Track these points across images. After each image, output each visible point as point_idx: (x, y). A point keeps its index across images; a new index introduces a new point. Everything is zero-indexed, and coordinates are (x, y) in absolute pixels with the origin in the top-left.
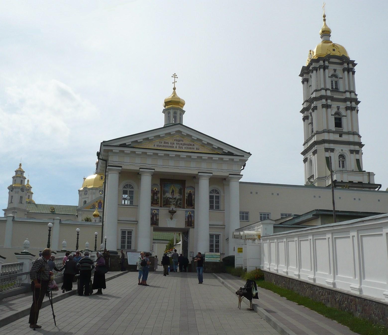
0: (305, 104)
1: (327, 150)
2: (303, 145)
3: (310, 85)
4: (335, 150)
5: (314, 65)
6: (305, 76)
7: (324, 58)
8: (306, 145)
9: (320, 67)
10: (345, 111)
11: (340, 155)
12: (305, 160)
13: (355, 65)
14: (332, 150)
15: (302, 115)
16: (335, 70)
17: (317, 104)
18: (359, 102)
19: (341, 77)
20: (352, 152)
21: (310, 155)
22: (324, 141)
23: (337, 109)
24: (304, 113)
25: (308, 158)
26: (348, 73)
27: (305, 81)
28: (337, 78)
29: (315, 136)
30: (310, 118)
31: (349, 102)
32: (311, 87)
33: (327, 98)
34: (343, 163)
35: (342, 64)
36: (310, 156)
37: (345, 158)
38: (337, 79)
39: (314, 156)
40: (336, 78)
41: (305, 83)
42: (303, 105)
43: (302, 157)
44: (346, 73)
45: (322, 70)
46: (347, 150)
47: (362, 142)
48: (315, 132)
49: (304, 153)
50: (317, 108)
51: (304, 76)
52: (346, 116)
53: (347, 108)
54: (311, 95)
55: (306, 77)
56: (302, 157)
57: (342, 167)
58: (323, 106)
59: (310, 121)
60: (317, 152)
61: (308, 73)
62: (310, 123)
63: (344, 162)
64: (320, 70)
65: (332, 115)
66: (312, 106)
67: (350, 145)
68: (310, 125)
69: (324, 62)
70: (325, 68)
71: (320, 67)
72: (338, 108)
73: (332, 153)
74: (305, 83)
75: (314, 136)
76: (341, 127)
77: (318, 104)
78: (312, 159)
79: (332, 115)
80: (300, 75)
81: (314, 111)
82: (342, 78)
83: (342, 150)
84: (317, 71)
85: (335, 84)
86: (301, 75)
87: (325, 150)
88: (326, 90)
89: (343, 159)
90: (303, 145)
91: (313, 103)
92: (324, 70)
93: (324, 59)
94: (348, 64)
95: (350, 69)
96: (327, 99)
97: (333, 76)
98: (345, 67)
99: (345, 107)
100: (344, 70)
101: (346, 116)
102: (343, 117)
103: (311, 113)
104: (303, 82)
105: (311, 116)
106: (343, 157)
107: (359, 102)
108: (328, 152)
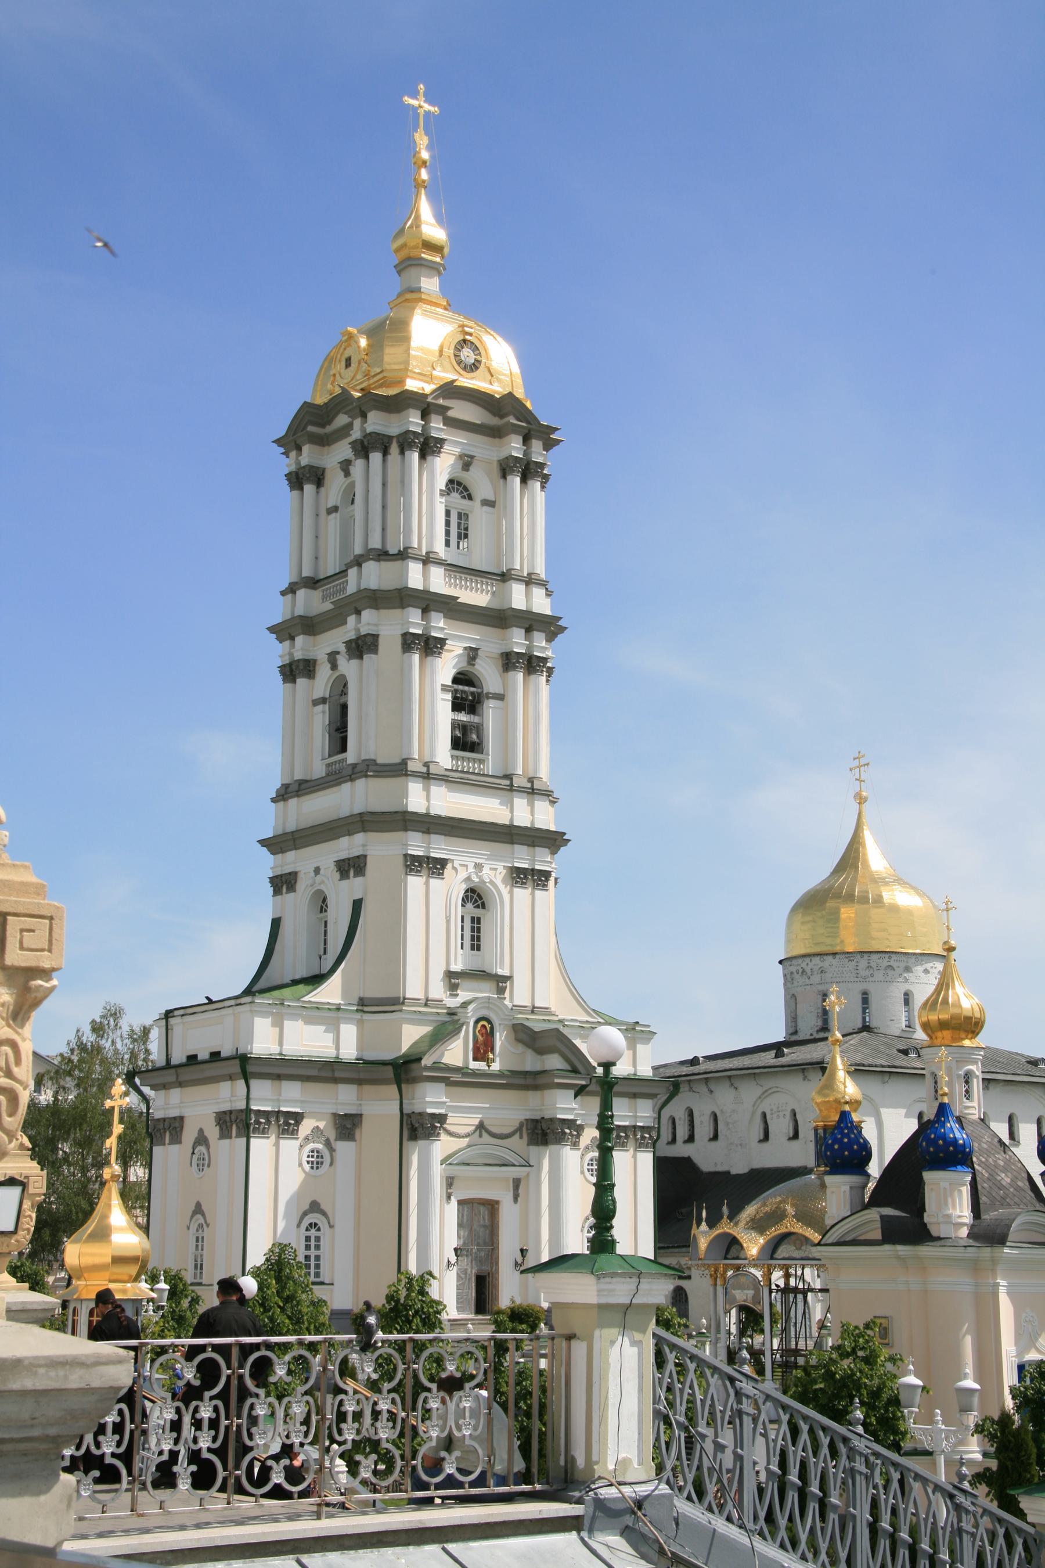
0: (301, 593)
1: (415, 864)
2: (273, 800)
3: (330, 504)
4: (449, 866)
5: (376, 422)
6: (308, 455)
8: (293, 802)
9: (406, 442)
10: (501, 669)
11: (467, 891)
12: (283, 883)
13: (549, 445)
14: (437, 866)
15: (277, 652)
16: (466, 462)
17: (376, 625)
18: (563, 629)
19: (491, 498)
20: (519, 876)
21: (316, 861)
22: (405, 821)
24: (292, 638)
25: (301, 876)
26: (524, 480)
27: (309, 481)
28: (470, 497)
29: (361, 783)
30: (324, 673)
31: (522, 632)
32: (333, 515)
33: (428, 602)
34: (476, 921)
35: (495, 433)
36: (317, 871)
37: (484, 900)
38: (466, 502)
39: (345, 883)
40: (464, 497)
41: (309, 488)
42: (289, 596)
43: (267, 864)
47: (565, 834)
48: (351, 756)
49: (275, 844)
50: (376, 646)
51: (306, 449)
52: (500, 697)
53: (508, 661)
54: (349, 566)
55: (316, 463)
56: (267, 864)
57: (472, 949)
58: (409, 642)
61: (324, 441)
62: (323, 701)
63: (479, 922)
64: (402, 452)
65: (444, 688)
66: (352, 620)
67: (512, 843)
68: (320, 707)
69: (425, 415)
70: (429, 447)
71: (406, 442)
72: (472, 654)
73: (434, 882)
74: (309, 488)
75: (351, 778)
76: (478, 752)
77: (389, 625)
78: (322, 887)
79: (444, 688)
80: (278, 442)
81: (361, 657)
83: (478, 867)
84: (385, 452)
85: (459, 524)
86: (290, 442)
88: (428, 560)
89: (478, 907)
90: (273, 800)
91: (358, 613)
92: (423, 456)
93: (429, 404)
94: (526, 440)
95: (532, 466)
96: (427, 606)
97: (454, 485)
98: (515, 454)
100: (505, 468)
101: (503, 695)
102: (488, 698)
103: (333, 657)
104: (296, 480)
105: (334, 667)
106: (480, 897)
107: (563, 629)
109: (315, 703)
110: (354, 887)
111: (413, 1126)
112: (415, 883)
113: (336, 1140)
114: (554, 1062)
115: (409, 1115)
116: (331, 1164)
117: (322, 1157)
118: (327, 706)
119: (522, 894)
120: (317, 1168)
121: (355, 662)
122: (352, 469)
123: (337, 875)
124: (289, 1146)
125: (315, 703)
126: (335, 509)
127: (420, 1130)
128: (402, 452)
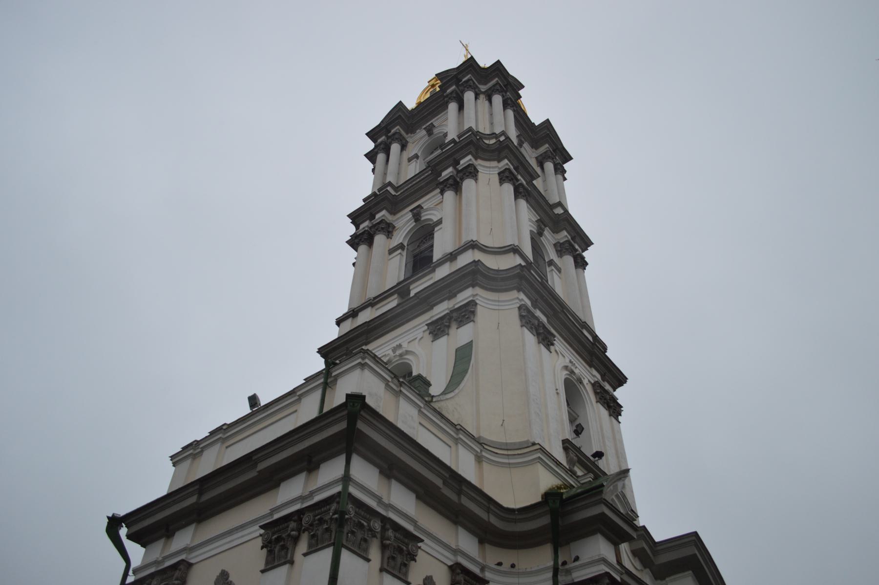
39: (443, 340)
45: (497, 99)
52: (559, 270)
53: (562, 249)
58: (505, 177)
59: (399, 237)
60: (473, 313)
62: (401, 246)
64: (490, 101)
67: (591, 366)
74: (395, 148)
87: (522, 317)
99: (555, 245)
109: (391, 251)
110: (461, 335)
118: (405, 253)
119: (604, 412)
121: (449, 195)
122: (436, 131)
123: (428, 338)
125: (391, 251)
126: (416, 156)
128: (490, 101)
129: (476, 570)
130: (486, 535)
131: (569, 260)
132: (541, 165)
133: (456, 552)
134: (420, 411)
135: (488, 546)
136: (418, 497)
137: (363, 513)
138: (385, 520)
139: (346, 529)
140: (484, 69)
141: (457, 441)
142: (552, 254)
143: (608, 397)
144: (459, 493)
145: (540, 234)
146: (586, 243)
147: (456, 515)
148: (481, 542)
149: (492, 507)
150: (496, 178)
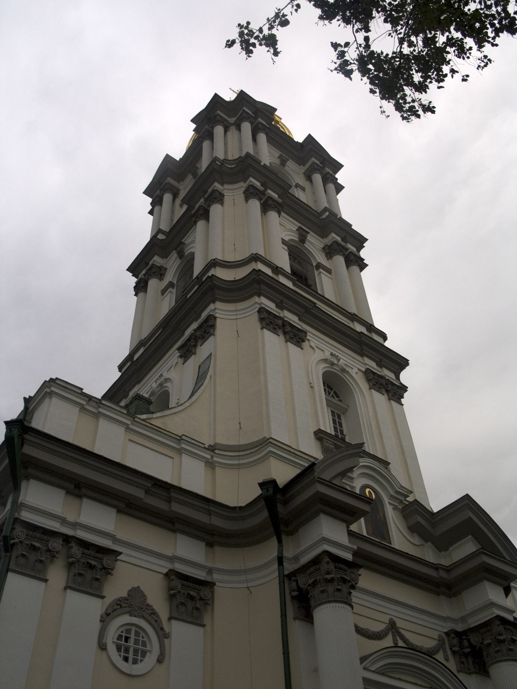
1: (269, 321)
7: (258, 106)
23: (297, 236)
41: (167, 198)
44: (317, 178)
46: (355, 370)
52: (329, 271)
59: (170, 277)
60: (213, 326)
62: (171, 285)
63: (339, 417)
64: (239, 128)
67: (362, 355)
82: (303, 189)
87: (261, 320)
99: (324, 249)
108: (274, 330)
111: (299, 589)
112: (273, 341)
113: (170, 619)
114: (467, 547)
115: (291, 576)
116: (160, 661)
117: (144, 644)
118: (174, 291)
120: (135, 662)
123: (181, 361)
124: (86, 608)
127: (315, 592)
129: (201, 575)
130: (212, 537)
131: (340, 260)
132: (309, 178)
133: (172, 559)
134: (128, 428)
135: (217, 549)
136: (119, 511)
137: (38, 535)
138: (67, 539)
139: (15, 553)
140: (227, 101)
141: (180, 451)
142: (320, 258)
143: (384, 381)
144: (169, 500)
145: (303, 239)
146: (360, 241)
147: (172, 523)
148: (210, 545)
149: (211, 508)
150: (242, 196)
